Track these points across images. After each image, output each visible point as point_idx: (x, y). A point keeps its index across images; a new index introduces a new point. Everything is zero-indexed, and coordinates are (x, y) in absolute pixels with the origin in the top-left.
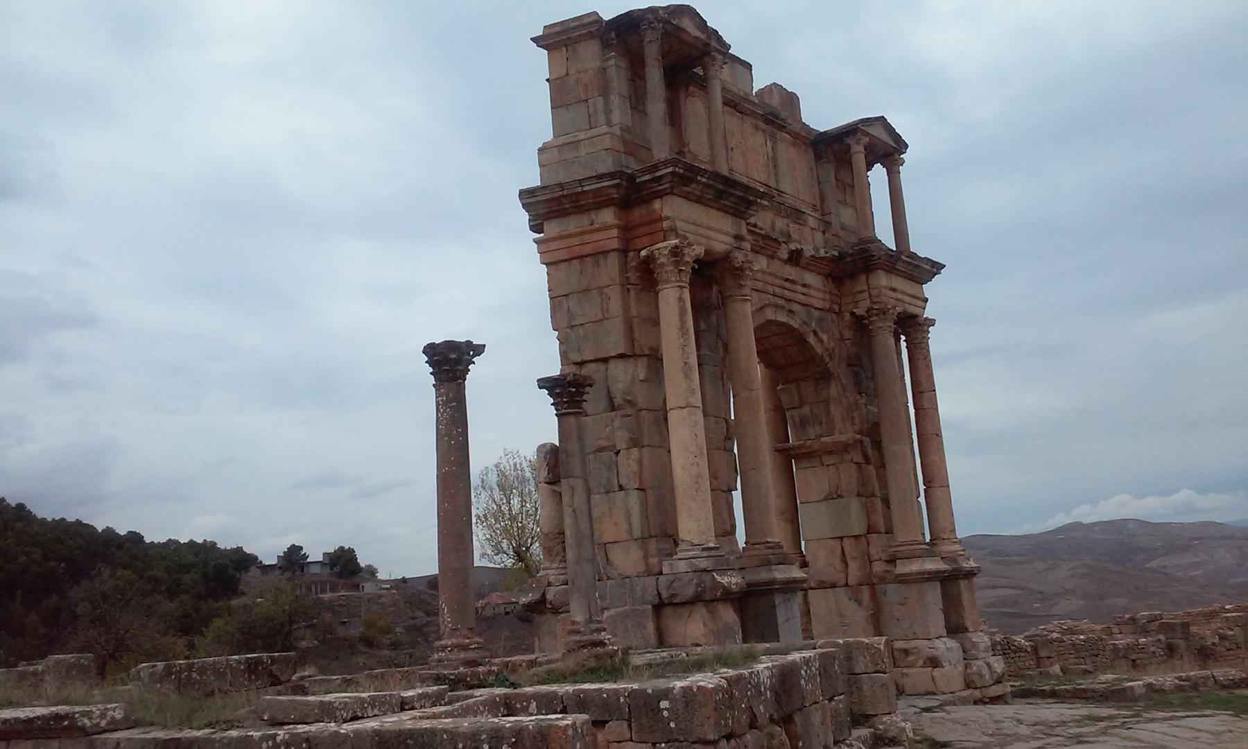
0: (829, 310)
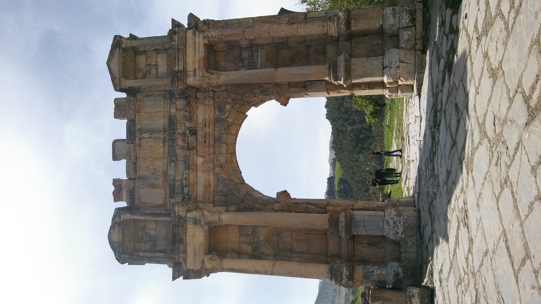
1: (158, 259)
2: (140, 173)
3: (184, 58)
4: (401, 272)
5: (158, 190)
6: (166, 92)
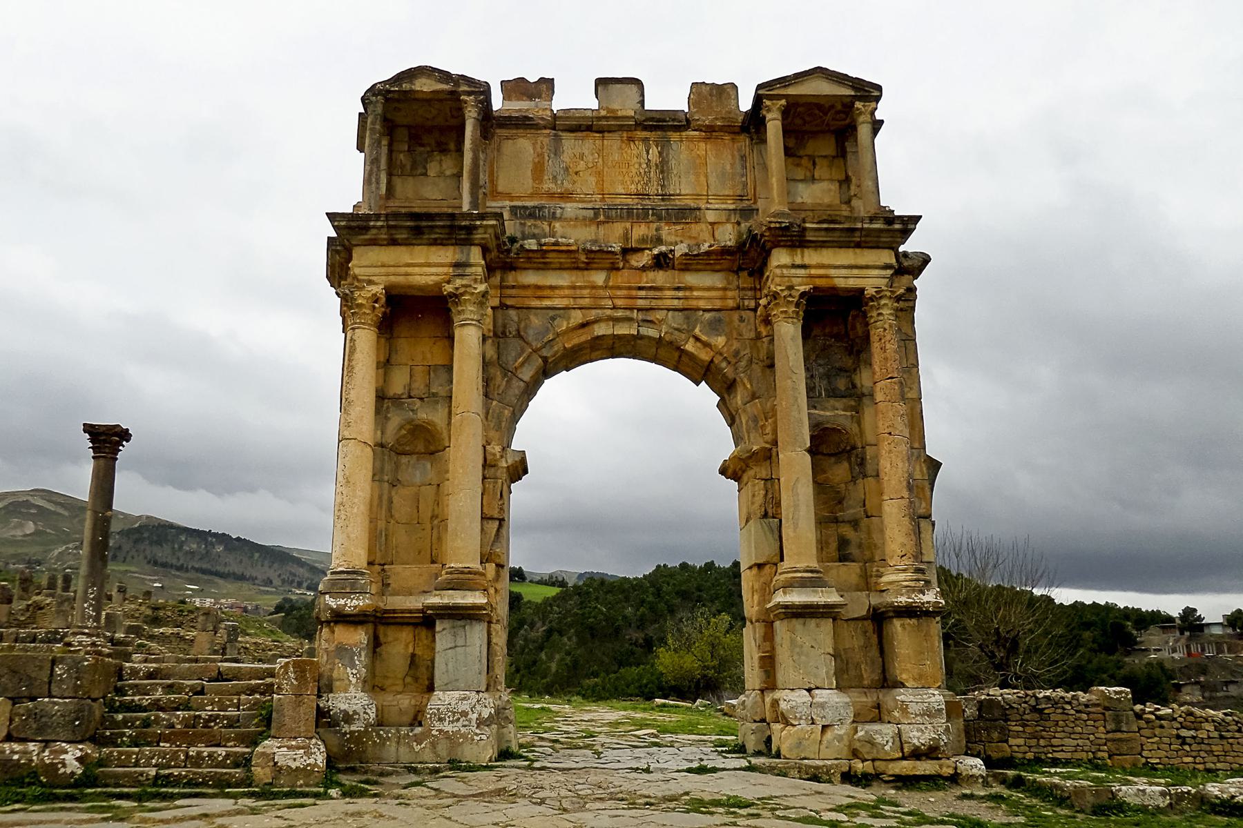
0: (738, 308)
1: (374, 180)
3: (833, 241)
4: (353, 728)
5: (531, 181)
6: (752, 202)
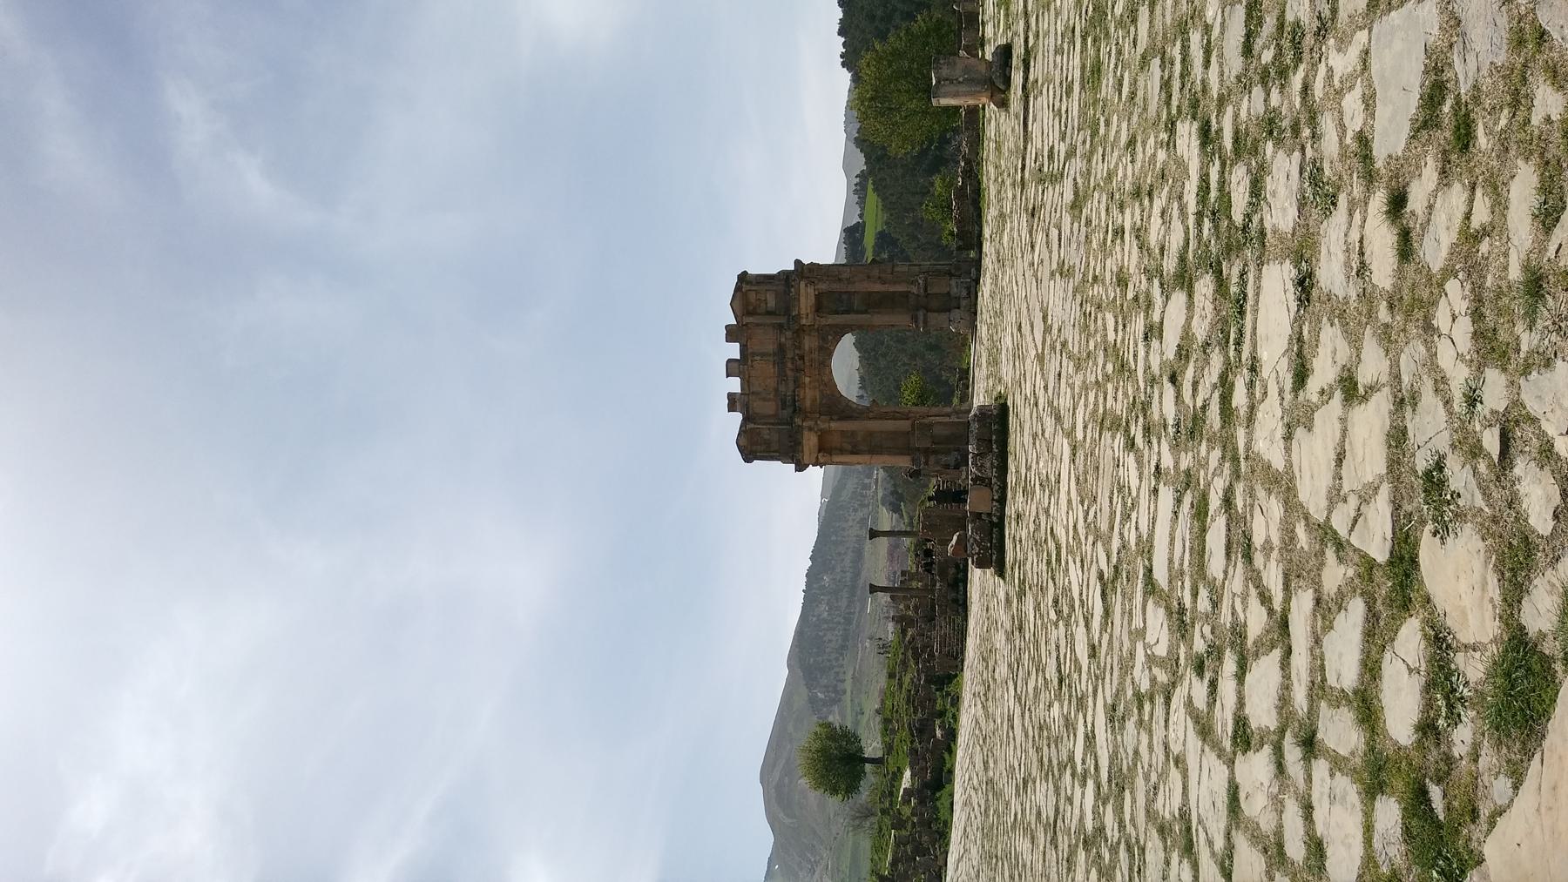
2: (754, 389)
